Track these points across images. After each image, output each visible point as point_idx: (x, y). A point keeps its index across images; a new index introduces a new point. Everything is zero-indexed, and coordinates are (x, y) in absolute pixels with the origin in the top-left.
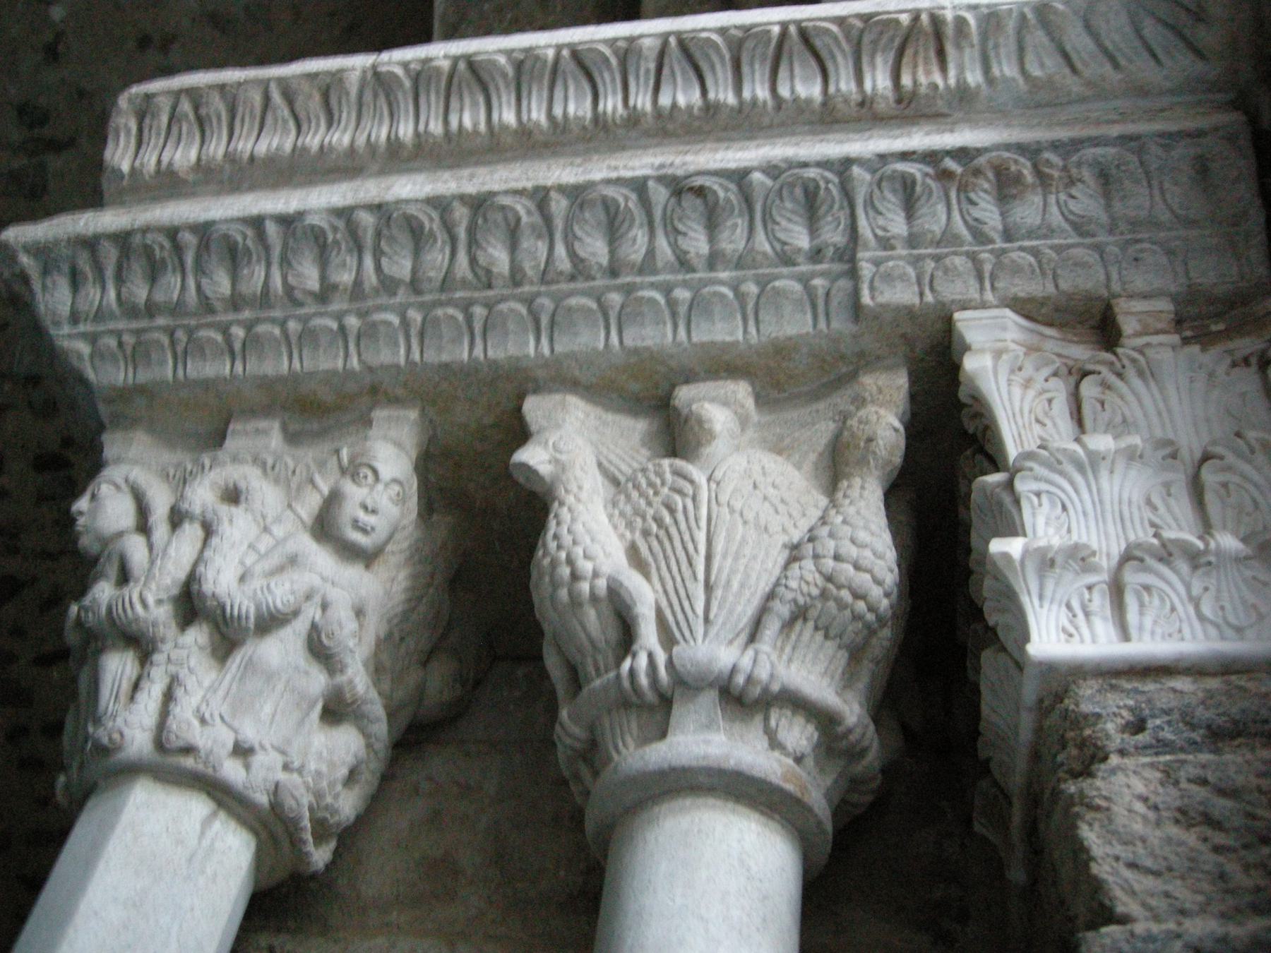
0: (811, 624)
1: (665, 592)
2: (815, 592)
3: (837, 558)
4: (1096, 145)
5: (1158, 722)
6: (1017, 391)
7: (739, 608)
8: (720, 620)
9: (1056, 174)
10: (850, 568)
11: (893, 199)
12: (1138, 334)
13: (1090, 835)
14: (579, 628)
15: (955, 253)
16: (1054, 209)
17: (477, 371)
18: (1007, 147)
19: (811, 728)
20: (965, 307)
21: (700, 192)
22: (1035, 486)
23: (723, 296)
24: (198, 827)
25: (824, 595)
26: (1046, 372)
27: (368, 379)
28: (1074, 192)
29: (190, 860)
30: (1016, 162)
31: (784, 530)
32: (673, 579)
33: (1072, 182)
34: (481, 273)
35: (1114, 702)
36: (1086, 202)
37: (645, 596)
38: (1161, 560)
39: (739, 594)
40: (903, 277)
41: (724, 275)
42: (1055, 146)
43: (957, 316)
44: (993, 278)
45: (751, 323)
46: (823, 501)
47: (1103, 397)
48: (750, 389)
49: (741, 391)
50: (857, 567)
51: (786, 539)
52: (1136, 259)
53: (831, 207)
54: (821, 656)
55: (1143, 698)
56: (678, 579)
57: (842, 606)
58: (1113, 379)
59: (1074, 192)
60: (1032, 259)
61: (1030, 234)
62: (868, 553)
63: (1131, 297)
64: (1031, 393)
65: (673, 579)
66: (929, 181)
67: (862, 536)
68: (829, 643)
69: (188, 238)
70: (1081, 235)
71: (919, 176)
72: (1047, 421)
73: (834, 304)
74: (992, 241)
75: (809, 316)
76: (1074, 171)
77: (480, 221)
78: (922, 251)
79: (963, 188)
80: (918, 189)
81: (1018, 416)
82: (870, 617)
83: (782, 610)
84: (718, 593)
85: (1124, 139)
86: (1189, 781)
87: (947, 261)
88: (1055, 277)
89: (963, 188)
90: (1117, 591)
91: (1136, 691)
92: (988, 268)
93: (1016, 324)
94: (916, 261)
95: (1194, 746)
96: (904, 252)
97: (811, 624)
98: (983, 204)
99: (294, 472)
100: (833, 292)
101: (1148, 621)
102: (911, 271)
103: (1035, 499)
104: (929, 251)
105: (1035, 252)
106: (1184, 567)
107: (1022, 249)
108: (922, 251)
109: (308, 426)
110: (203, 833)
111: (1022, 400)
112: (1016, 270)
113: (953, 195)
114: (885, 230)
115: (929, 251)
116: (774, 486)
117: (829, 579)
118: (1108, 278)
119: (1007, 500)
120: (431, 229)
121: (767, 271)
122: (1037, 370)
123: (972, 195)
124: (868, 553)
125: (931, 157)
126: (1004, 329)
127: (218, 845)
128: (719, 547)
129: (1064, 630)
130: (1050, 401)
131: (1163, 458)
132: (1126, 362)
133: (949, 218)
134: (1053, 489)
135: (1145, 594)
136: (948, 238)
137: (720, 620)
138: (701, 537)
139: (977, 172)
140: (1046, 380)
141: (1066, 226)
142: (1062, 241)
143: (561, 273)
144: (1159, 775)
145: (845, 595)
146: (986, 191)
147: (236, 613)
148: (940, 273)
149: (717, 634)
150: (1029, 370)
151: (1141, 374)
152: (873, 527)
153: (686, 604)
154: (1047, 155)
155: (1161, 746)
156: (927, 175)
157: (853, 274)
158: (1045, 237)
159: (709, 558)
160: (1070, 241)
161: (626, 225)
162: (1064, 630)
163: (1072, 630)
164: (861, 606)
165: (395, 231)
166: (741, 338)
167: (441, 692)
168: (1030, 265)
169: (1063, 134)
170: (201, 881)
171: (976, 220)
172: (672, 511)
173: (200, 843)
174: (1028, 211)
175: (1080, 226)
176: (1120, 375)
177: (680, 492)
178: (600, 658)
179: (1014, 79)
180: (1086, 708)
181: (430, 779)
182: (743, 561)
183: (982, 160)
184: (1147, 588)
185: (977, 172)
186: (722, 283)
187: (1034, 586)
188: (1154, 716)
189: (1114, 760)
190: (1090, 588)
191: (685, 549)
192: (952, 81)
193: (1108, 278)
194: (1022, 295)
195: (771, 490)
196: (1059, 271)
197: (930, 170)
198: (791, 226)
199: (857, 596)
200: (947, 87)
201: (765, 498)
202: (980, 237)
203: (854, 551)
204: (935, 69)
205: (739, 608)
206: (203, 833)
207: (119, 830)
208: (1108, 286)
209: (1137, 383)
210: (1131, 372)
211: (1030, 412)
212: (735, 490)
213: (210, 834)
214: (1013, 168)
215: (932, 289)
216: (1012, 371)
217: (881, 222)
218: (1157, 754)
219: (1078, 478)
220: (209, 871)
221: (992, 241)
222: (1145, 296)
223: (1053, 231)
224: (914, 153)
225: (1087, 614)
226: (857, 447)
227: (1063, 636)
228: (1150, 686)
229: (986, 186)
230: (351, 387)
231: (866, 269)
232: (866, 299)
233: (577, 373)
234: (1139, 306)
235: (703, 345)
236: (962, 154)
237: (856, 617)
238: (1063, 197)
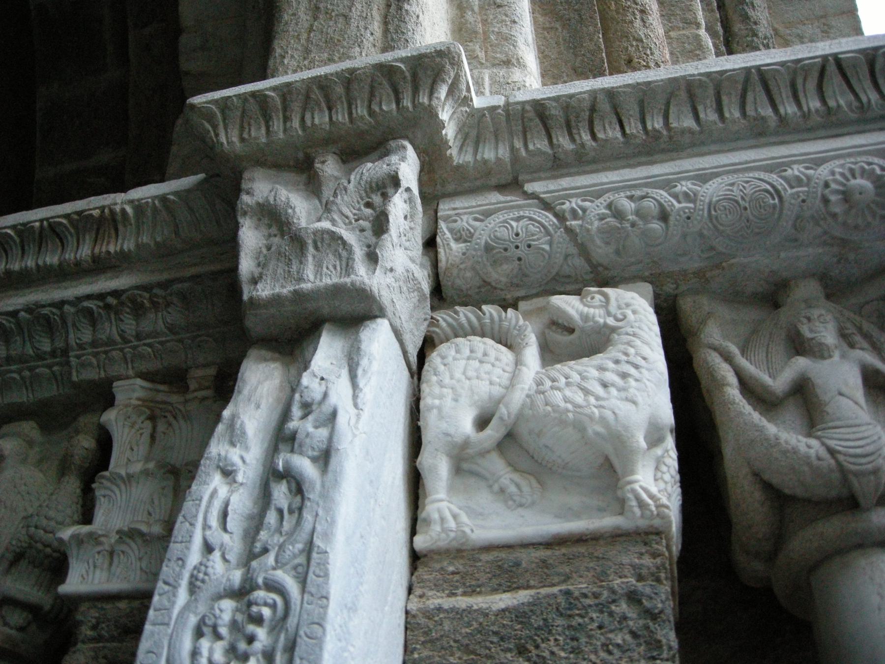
0: (27, 560)
2: (25, 545)
3: (36, 527)
4: (182, 282)
5: (104, 625)
6: (126, 430)
9: (160, 301)
10: (42, 532)
11: (86, 321)
15: (113, 350)
16: (160, 322)
18: (137, 287)
19: (25, 614)
20: (119, 378)
22: (103, 492)
23: (14, 379)
25: (30, 547)
26: (143, 418)
28: (169, 310)
30: (141, 296)
31: (25, 510)
33: (168, 304)
35: (94, 613)
36: (174, 315)
38: (130, 537)
40: (90, 364)
41: (13, 367)
42: (160, 285)
44: (132, 361)
45: (30, 391)
48: (35, 425)
49: (29, 428)
50: (46, 531)
51: (25, 514)
55: (103, 612)
57: (39, 552)
58: (171, 419)
59: (169, 310)
60: (150, 350)
61: (148, 336)
62: (53, 523)
63: (197, 367)
64: (133, 431)
66: (101, 311)
67: (52, 513)
68: (36, 570)
70: (174, 334)
71: (94, 308)
72: (135, 449)
74: (131, 342)
75: (55, 387)
76: (169, 298)
78: (99, 349)
80: (96, 315)
82: (55, 555)
83: (10, 556)
85: (193, 278)
86: (103, 657)
87: (109, 354)
88: (162, 359)
89: (116, 313)
90: (112, 554)
91: (102, 609)
92: (129, 356)
93: (142, 387)
94: (95, 355)
95: (112, 639)
96: (90, 350)
97: (27, 560)
98: (126, 321)
101: (119, 570)
102: (94, 361)
103: (102, 499)
104: (102, 349)
105: (150, 345)
106: (139, 541)
107: (145, 345)
108: (99, 349)
112: (142, 357)
113: (113, 316)
114: (79, 339)
115: (102, 349)
116: (25, 485)
117: (31, 537)
121: (32, 364)
122: (139, 416)
123: (122, 317)
124: (53, 523)
125: (101, 296)
126: (134, 391)
129: (82, 576)
130: (141, 434)
131: (164, 473)
134: (112, 494)
135: (122, 556)
136: (110, 342)
139: (122, 304)
141: (166, 330)
142: (164, 339)
144: (92, 654)
145: (40, 546)
146: (128, 313)
148: (107, 361)
150: (134, 417)
151: (184, 417)
152: (60, 507)
154: (156, 291)
155: (99, 639)
156: (99, 307)
158: (155, 337)
160: (168, 338)
162: (82, 576)
163: (85, 576)
164: (48, 550)
166: (25, 400)
168: (149, 354)
169: (165, 276)
171: (122, 331)
174: (147, 325)
175: (172, 329)
176: (175, 418)
179: (147, 244)
180: (79, 617)
183: (124, 297)
184: (123, 552)
185: (122, 304)
186: (14, 372)
187: (75, 552)
188: (103, 623)
189: (80, 646)
190: (99, 553)
192: (118, 249)
194: (144, 370)
195: (23, 487)
196: (163, 356)
197: (101, 304)
198: (41, 339)
199: (46, 546)
200: (116, 251)
201: (19, 493)
202: (125, 340)
203: (44, 522)
204: (113, 240)
209: (182, 422)
210: (180, 418)
214: (139, 300)
215: (105, 371)
216: (125, 420)
217: (79, 336)
218: (98, 642)
219: (123, 487)
221: (131, 342)
222: (204, 366)
223: (158, 333)
224: (92, 295)
225: (95, 567)
227: (81, 578)
228: (108, 606)
229: (128, 310)
231: (73, 361)
234: (199, 373)
235: (9, 404)
236: (116, 293)
237: (47, 556)
238: (165, 313)
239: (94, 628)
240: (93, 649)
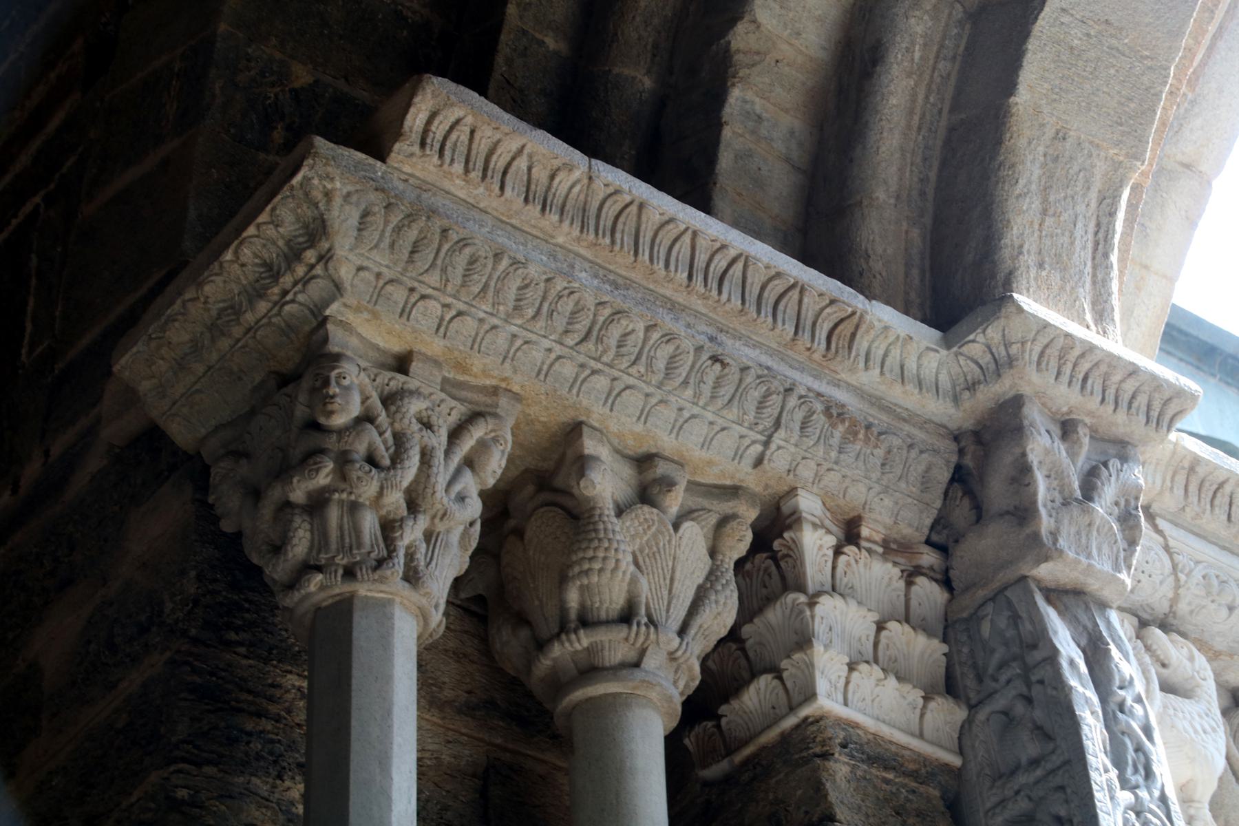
12: (868, 540)
13: (828, 785)
21: (724, 365)
34: (600, 348)
37: (645, 589)
43: (800, 492)
46: (710, 562)
58: (853, 562)
69: (454, 237)
73: (748, 452)
79: (833, 426)
80: (815, 416)
84: (674, 601)
119: (808, 613)
128: (678, 575)
133: (819, 438)
138: (670, 564)
151: (865, 565)
155: (852, 757)
157: (766, 444)
159: (672, 580)
172: (657, 544)
177: (662, 533)
231: (773, 446)
232: (766, 462)
239: (844, 746)
240: (848, 764)
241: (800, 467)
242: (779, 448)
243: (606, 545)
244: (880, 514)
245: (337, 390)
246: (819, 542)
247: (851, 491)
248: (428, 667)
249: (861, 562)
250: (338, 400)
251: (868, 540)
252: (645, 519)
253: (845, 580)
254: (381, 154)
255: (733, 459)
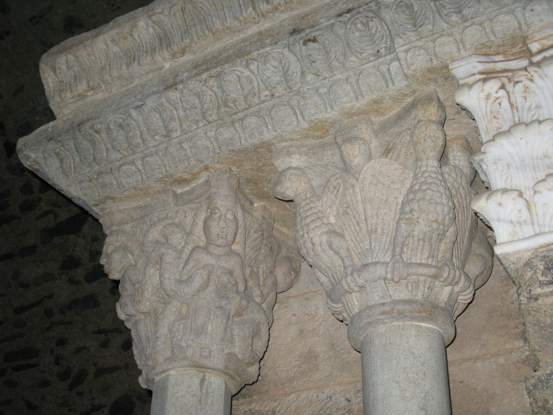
1: (352, 240)
6: (483, 103)
7: (384, 240)
8: (377, 247)
12: (540, 52)
14: (321, 263)
17: (246, 148)
24: (198, 385)
27: (201, 165)
29: (200, 401)
32: (353, 233)
39: (383, 233)
47: (524, 95)
52: (532, 10)
53: (377, 28)
54: (425, 251)
56: (356, 234)
58: (528, 83)
64: (490, 101)
65: (353, 233)
77: (223, 83)
81: (485, 118)
99: (186, 217)
100: (391, 69)
109: (185, 189)
110: (201, 389)
111: (486, 106)
118: (519, 24)
120: (202, 92)
127: (210, 390)
128: (369, 213)
130: (500, 104)
132: (533, 73)
137: (377, 247)
140: (497, 92)
143: (266, 96)
147: (183, 295)
149: (377, 255)
151: (541, 77)
153: (361, 244)
161: (287, 64)
165: (188, 98)
167: (285, 280)
170: (208, 408)
173: (201, 392)
176: (531, 80)
178: (334, 274)
181: (294, 315)
182: (380, 217)
191: (354, 217)
193: (519, 24)
205: (384, 240)
206: (201, 389)
207: (168, 399)
208: (520, 29)
211: (491, 112)
212: (371, 183)
213: (204, 387)
220: (209, 402)
226: (420, 143)
230: (196, 170)
233: (290, 136)
241: (437, 49)
242: (407, 51)
243: (301, 233)
244: (542, 20)
245: (105, 260)
246: (483, 95)
247: (498, 28)
248: (339, 342)
249: (536, 78)
250: (106, 266)
251: (540, 52)
252: (334, 187)
253: (528, 104)
254: (51, 116)
255: (388, 86)
